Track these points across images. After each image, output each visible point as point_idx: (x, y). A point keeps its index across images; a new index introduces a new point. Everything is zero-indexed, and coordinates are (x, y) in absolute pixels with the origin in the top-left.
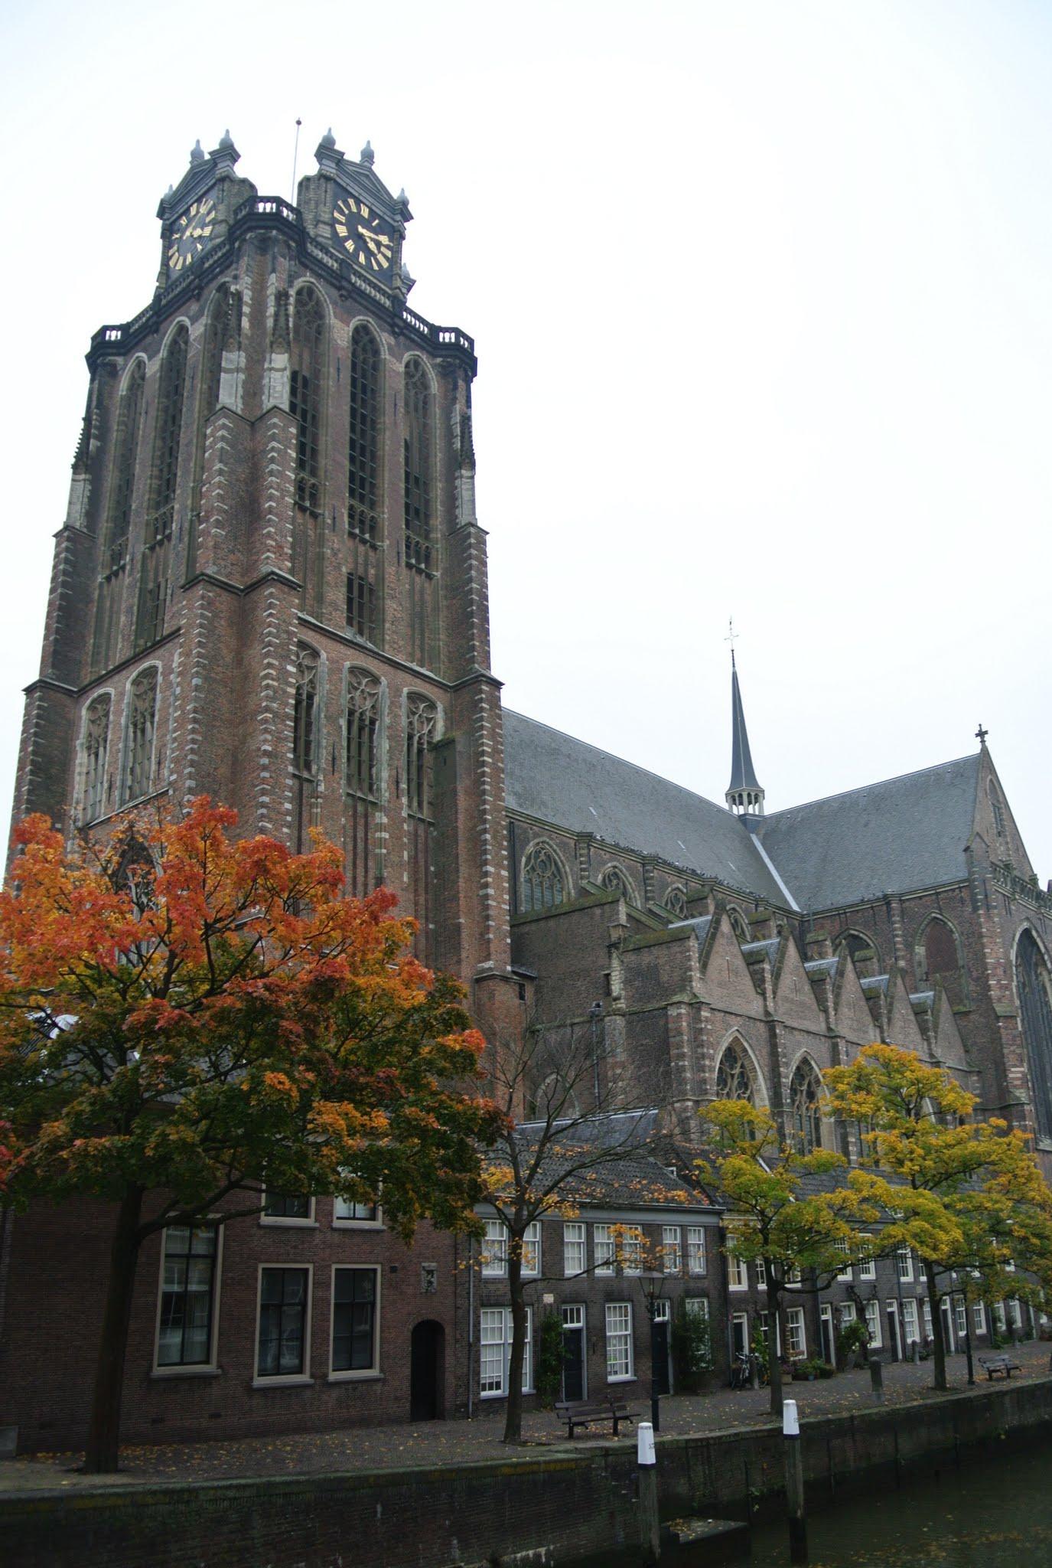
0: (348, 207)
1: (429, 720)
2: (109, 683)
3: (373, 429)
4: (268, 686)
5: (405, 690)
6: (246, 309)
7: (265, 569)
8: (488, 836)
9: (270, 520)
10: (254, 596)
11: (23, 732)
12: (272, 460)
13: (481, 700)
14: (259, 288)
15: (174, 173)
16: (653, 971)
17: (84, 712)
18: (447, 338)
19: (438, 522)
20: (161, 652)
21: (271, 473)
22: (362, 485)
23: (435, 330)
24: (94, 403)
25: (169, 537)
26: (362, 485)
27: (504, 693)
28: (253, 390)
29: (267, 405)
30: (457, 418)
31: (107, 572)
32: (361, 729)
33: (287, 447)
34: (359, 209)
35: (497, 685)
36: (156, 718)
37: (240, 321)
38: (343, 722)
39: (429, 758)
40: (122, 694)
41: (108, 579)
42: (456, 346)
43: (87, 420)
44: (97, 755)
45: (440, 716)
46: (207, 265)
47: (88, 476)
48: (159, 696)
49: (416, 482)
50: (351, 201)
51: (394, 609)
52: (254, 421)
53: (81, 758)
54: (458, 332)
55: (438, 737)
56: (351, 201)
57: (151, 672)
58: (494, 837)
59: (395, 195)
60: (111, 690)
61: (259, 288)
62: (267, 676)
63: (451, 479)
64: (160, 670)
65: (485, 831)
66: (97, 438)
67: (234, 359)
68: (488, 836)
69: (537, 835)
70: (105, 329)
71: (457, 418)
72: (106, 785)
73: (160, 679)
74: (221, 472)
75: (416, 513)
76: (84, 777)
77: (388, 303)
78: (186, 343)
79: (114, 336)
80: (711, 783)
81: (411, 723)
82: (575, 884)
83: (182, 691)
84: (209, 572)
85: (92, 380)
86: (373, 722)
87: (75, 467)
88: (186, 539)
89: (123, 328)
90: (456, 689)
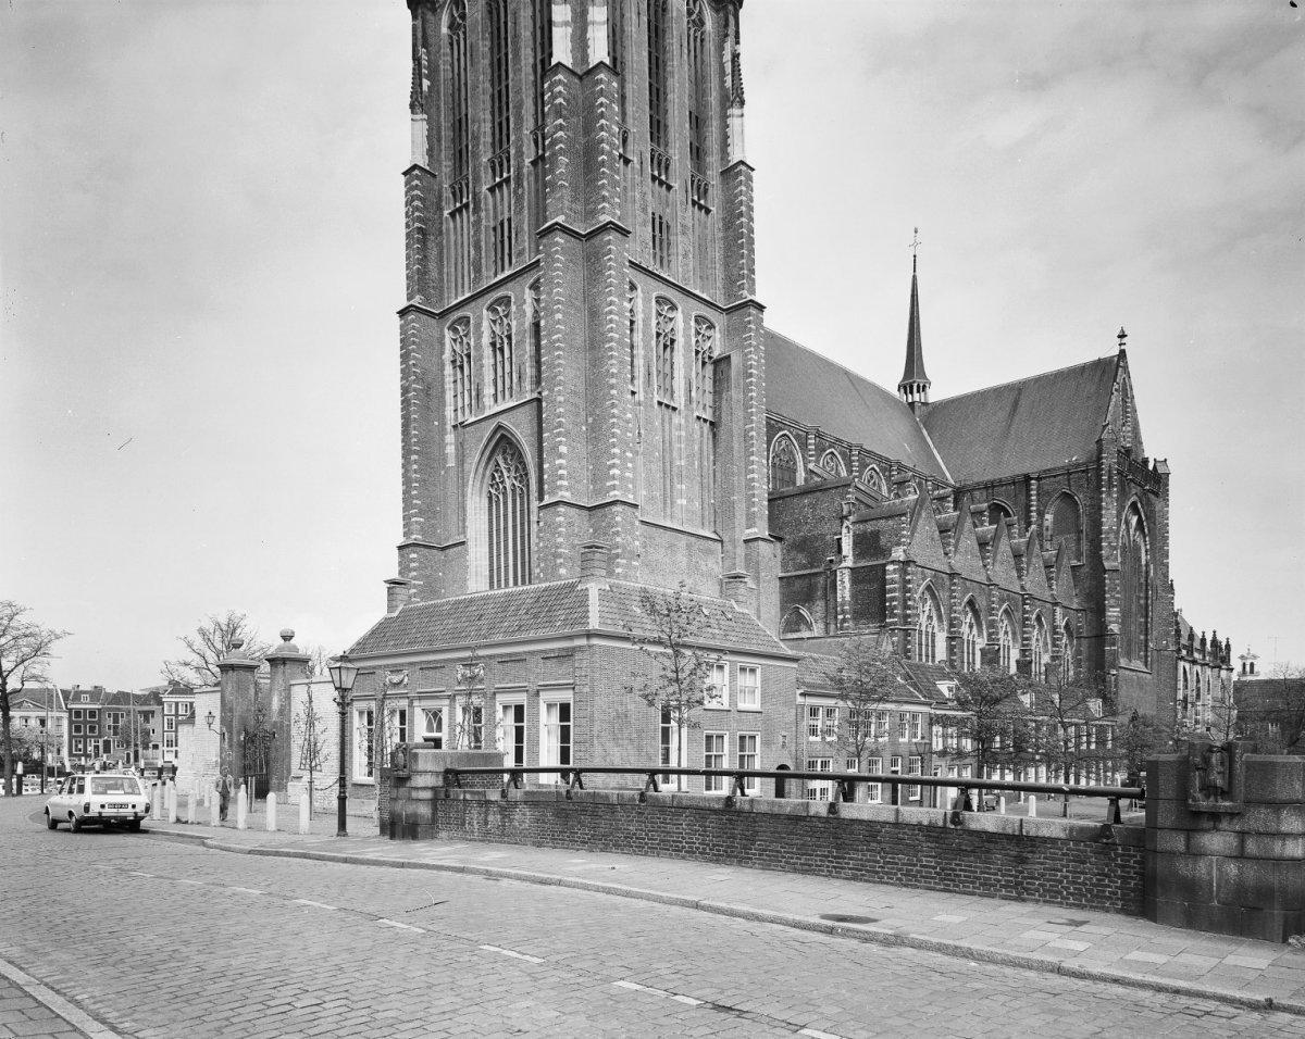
1: (709, 338)
2: (466, 308)
4: (611, 321)
7: (605, 218)
8: (754, 433)
9: (603, 173)
10: (596, 241)
11: (402, 349)
12: (602, 115)
13: (749, 322)
17: (446, 330)
20: (510, 285)
21: (602, 128)
25: (507, 180)
27: (766, 315)
28: (581, 43)
29: (593, 61)
31: (453, 208)
32: (665, 347)
33: (611, 102)
35: (761, 308)
36: (514, 342)
38: (654, 343)
40: (480, 317)
41: (452, 215)
43: (416, 59)
44: (462, 368)
45: (717, 335)
47: (425, 116)
48: (514, 324)
53: (448, 369)
55: (715, 355)
57: (506, 301)
58: (758, 434)
60: (469, 314)
62: (611, 312)
64: (513, 300)
65: (752, 429)
66: (428, 77)
68: (754, 433)
69: (781, 429)
72: (474, 393)
73: (513, 308)
74: (561, 127)
76: (452, 385)
81: (697, 341)
83: (547, 322)
84: (560, 219)
85: (415, 17)
86: (673, 341)
87: (412, 106)
90: (728, 311)
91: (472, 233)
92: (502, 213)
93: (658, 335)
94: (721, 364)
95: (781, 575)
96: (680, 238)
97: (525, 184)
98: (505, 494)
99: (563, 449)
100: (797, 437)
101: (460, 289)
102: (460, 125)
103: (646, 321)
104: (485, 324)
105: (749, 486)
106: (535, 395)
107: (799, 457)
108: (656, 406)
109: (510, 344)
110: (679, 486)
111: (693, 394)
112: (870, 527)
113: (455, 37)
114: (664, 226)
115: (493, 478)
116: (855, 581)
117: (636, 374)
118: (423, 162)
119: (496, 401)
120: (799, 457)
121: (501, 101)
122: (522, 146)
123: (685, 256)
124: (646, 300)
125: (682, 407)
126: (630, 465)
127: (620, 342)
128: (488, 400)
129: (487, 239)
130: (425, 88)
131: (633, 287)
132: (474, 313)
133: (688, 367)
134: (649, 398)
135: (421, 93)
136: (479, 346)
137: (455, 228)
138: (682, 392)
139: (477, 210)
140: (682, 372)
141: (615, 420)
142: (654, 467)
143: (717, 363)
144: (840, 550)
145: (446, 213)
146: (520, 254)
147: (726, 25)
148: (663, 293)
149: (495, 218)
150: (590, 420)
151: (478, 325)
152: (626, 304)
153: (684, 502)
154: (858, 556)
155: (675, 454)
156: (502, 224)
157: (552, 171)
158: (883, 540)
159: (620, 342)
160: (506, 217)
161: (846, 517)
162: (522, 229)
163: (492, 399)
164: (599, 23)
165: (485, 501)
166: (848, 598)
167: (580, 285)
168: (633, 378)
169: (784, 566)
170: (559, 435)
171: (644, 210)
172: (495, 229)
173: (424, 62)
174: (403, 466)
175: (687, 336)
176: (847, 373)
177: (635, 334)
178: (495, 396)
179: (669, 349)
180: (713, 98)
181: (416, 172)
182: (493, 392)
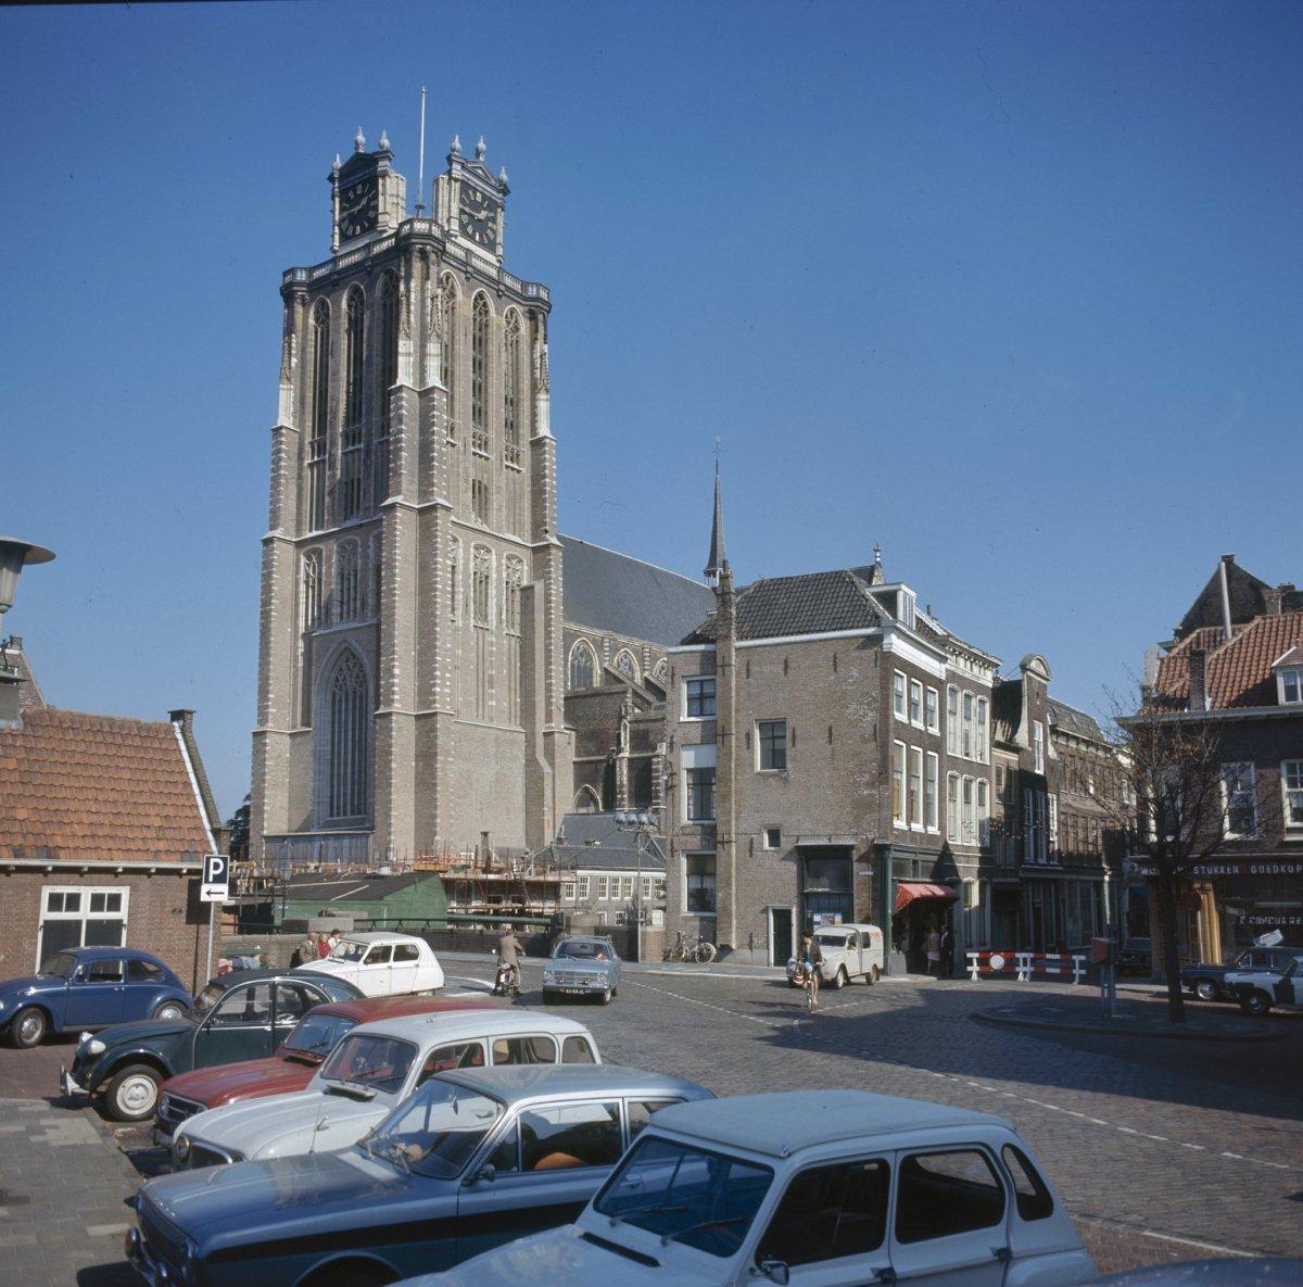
0: (468, 196)
3: (486, 370)
5: (505, 554)
6: (412, 308)
16: (646, 733)
19: (525, 431)
22: (479, 414)
26: (479, 414)
34: (475, 197)
36: (359, 576)
37: (408, 317)
39: (518, 593)
49: (512, 403)
50: (471, 192)
51: (497, 500)
52: (426, 394)
55: (525, 583)
56: (471, 192)
64: (360, 543)
67: (405, 346)
69: (579, 637)
70: (292, 271)
75: (512, 425)
77: (493, 273)
82: (601, 664)
84: (399, 499)
86: (487, 577)
89: (310, 271)
92: (353, 473)
93: (475, 573)
94: (527, 592)
95: (575, 759)
96: (495, 497)
97: (373, 458)
98: (347, 694)
100: (594, 642)
103: (466, 565)
106: (374, 621)
108: (472, 629)
109: (356, 576)
110: (490, 691)
111: (504, 617)
112: (642, 726)
114: (483, 490)
115: (337, 680)
116: (630, 768)
117: (456, 606)
119: (341, 619)
122: (371, 429)
123: (499, 509)
124: (466, 549)
125: (494, 628)
126: (448, 683)
127: (445, 592)
128: (335, 619)
131: (455, 540)
132: (326, 547)
133: (499, 596)
134: (466, 626)
135: (290, 368)
138: (494, 617)
140: (495, 601)
142: (468, 678)
143: (523, 590)
144: (619, 743)
146: (367, 509)
147: (536, 331)
148: (479, 542)
152: (448, 562)
153: (494, 703)
154: (633, 749)
155: (487, 664)
156: (352, 481)
158: (651, 738)
159: (442, 591)
160: (356, 476)
161: (624, 717)
162: (369, 491)
164: (434, 355)
165: (329, 698)
166: (625, 782)
168: (453, 610)
169: (578, 754)
171: (466, 481)
172: (346, 484)
174: (260, 665)
175: (499, 572)
177: (456, 576)
178: (341, 614)
179: (484, 583)
180: (525, 385)
182: (339, 611)
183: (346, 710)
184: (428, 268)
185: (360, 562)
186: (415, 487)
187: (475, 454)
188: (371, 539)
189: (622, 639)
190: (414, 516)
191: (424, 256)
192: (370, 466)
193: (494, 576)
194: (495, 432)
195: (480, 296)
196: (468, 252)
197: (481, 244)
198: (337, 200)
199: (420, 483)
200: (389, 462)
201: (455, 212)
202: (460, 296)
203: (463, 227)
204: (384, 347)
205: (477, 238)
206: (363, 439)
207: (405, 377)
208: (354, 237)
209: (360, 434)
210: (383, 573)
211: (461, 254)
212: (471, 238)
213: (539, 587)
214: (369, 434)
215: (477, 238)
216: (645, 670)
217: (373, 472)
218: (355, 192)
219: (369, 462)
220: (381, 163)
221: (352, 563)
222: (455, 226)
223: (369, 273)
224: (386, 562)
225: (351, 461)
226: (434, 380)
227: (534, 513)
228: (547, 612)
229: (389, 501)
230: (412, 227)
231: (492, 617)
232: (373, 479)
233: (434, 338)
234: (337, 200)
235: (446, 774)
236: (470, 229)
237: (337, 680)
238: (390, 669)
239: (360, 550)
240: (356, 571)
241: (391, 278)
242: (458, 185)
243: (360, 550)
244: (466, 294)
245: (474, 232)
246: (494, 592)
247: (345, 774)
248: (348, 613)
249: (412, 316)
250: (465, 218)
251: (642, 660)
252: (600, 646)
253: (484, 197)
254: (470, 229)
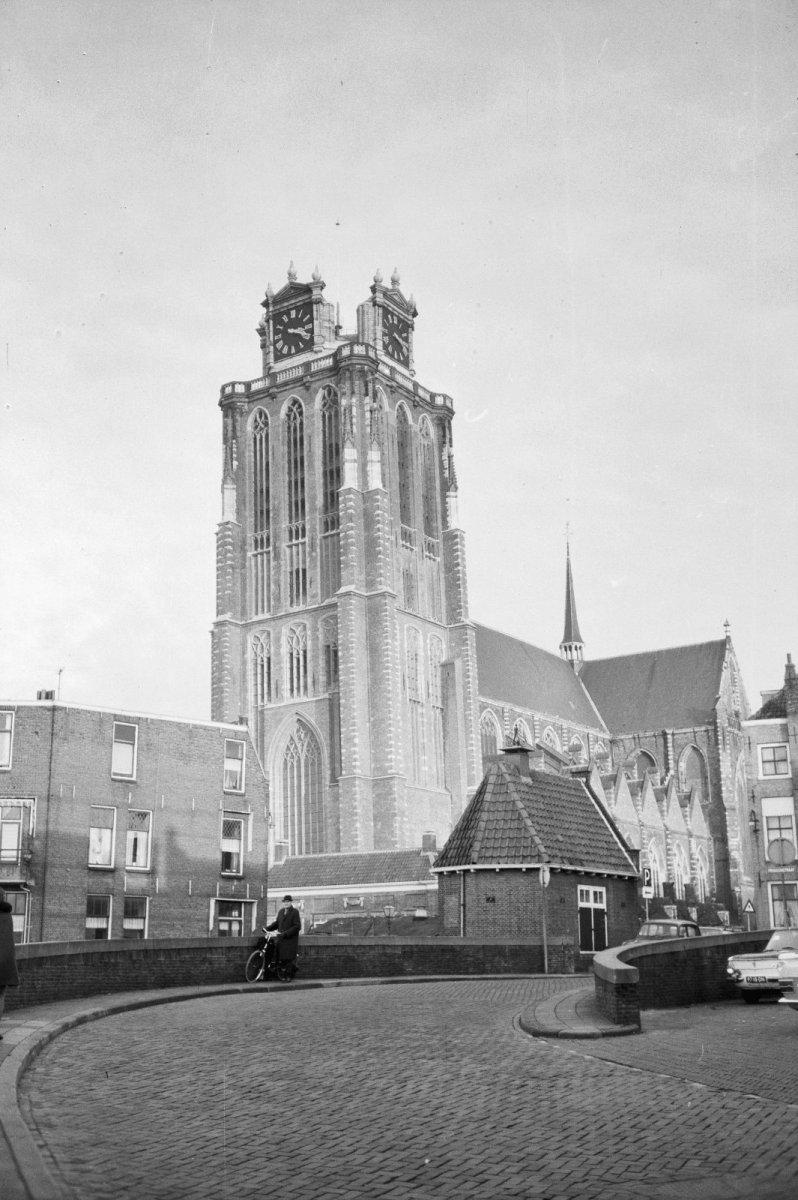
6: (354, 420)
14: (361, 405)
15: (279, 285)
18: (439, 401)
21: (379, 530)
23: (433, 396)
24: (230, 434)
30: (445, 457)
36: (309, 656)
39: (439, 669)
42: (444, 407)
46: (314, 368)
49: (428, 499)
51: (422, 587)
52: (368, 496)
54: (445, 397)
55: (443, 659)
59: (407, 299)
61: (361, 405)
63: (444, 497)
67: (349, 453)
70: (233, 384)
71: (445, 457)
74: (352, 528)
77: (410, 386)
78: (301, 414)
79: (240, 389)
80: (548, 638)
84: (351, 588)
85: (225, 416)
86: (416, 655)
88: (318, 550)
89: (248, 385)
91: (272, 573)
98: (299, 761)
99: (356, 741)
100: (497, 712)
101: (260, 609)
102: (263, 494)
104: (284, 640)
105: (469, 754)
106: (326, 696)
107: (498, 726)
113: (258, 437)
118: (232, 517)
120: (498, 726)
121: (297, 485)
123: (423, 595)
129: (285, 580)
130: (235, 467)
136: (278, 654)
137: (256, 565)
139: (277, 557)
141: (391, 722)
143: (444, 666)
145: (249, 554)
149: (292, 565)
150: (372, 719)
151: (278, 640)
157: (345, 554)
163: (289, 691)
167: (364, 628)
170: (354, 731)
173: (234, 449)
175: (425, 651)
176: (522, 644)
181: (229, 526)
183: (299, 776)
184: (366, 385)
185: (309, 643)
186: (363, 577)
187: (403, 546)
188: (319, 623)
189: (518, 710)
190: (364, 602)
191: (363, 373)
192: (316, 558)
193: (421, 653)
194: (417, 528)
195: (401, 407)
196: (392, 369)
197: (399, 361)
198: (271, 322)
199: (368, 574)
200: (339, 554)
201: (379, 335)
202: (387, 408)
203: (385, 347)
204: (324, 453)
205: (396, 357)
206: (307, 533)
207: (350, 479)
208: (289, 355)
209: (304, 530)
210: (340, 654)
211: (387, 372)
212: (391, 356)
213: (458, 663)
214: (313, 529)
215: (396, 357)
216: (536, 737)
217: (319, 564)
218: (288, 315)
219: (314, 554)
220: (315, 292)
221: (302, 644)
222: (380, 346)
223: (307, 388)
224: (342, 644)
225: (294, 553)
226: (375, 483)
227: (448, 598)
228: (466, 686)
229: (343, 590)
230: (352, 351)
231: (422, 691)
232: (319, 569)
233: (375, 446)
234: (271, 322)
235: (403, 833)
236: (390, 349)
237: (288, 748)
238: (350, 740)
239: (309, 633)
240: (305, 652)
241: (329, 394)
242: (381, 311)
243: (309, 633)
244: (392, 406)
245: (393, 351)
246: (423, 669)
247: (300, 833)
248: (298, 689)
249: (354, 427)
250: (386, 339)
251: (533, 728)
252: (501, 716)
253: (400, 320)
254: (390, 349)
